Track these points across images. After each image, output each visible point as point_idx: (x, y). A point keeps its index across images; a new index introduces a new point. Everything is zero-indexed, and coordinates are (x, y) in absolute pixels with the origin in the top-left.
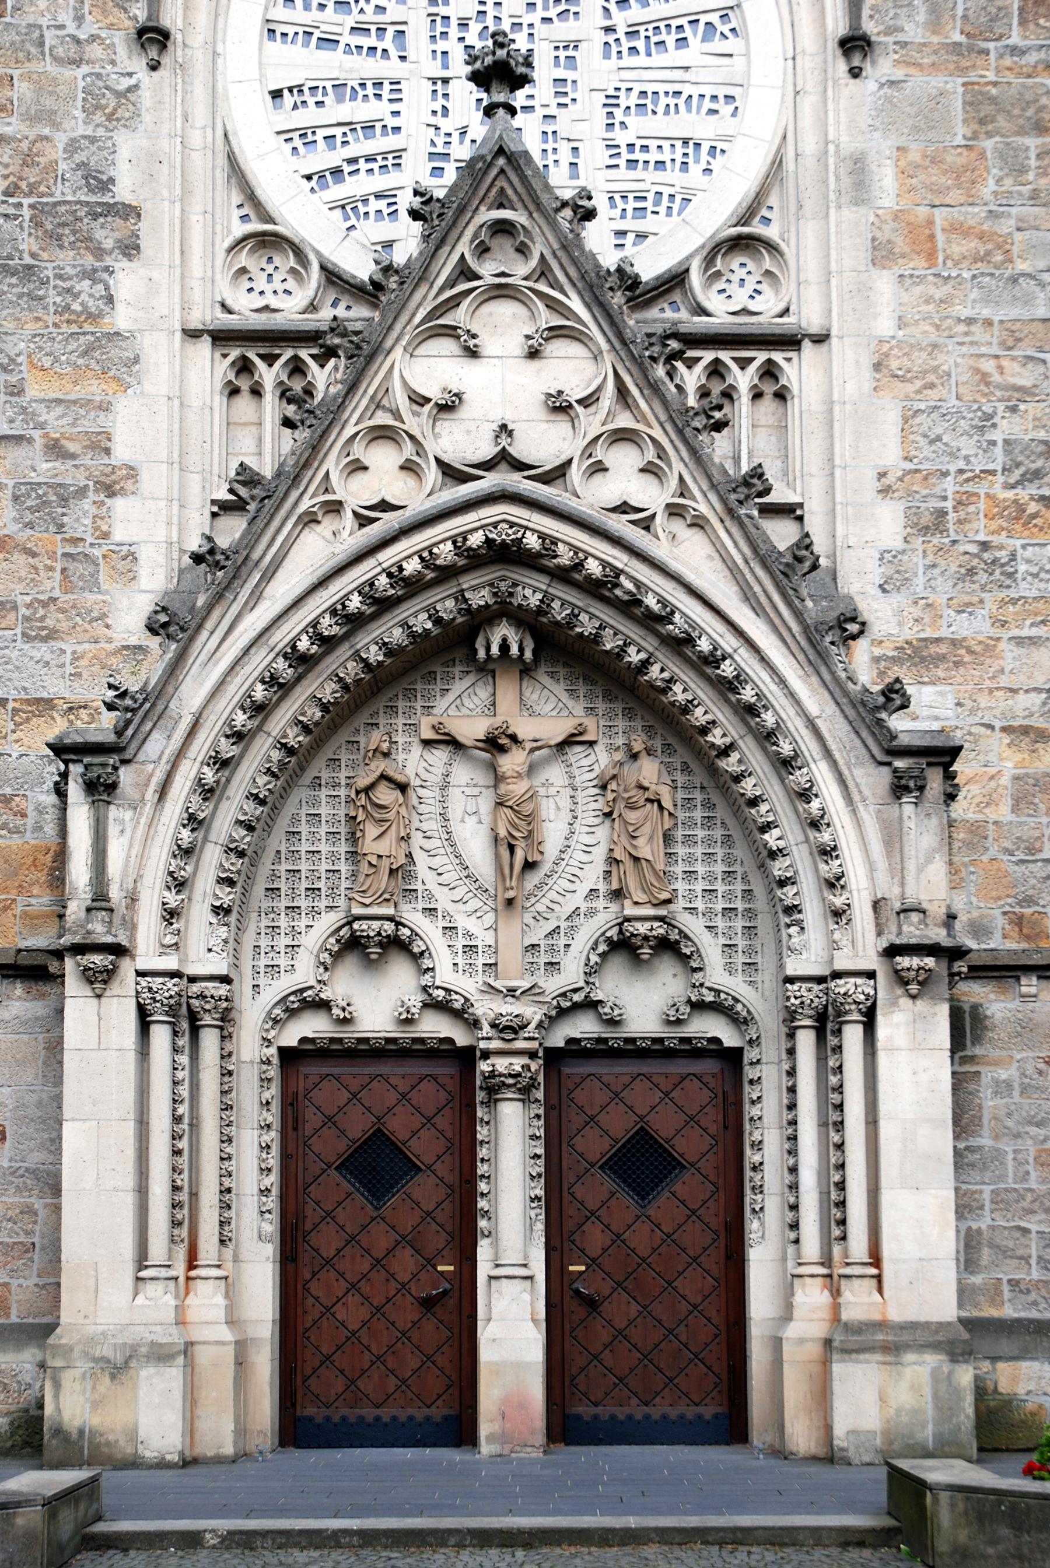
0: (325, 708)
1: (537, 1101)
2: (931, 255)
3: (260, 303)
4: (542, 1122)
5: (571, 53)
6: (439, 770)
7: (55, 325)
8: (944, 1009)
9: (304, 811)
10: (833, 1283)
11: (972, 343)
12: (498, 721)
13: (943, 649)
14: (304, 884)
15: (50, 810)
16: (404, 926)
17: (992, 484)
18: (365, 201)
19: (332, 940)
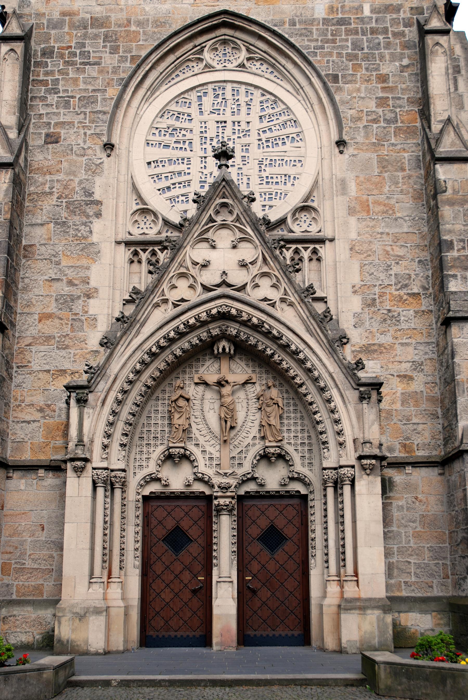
0: (161, 372)
1: (234, 515)
2: (368, 211)
3: (142, 232)
4: (236, 523)
5: (247, 147)
6: (200, 393)
7: (72, 241)
8: (379, 479)
9: (153, 409)
10: (341, 583)
11: (383, 241)
12: (221, 376)
13: (376, 347)
14: (153, 435)
15: (64, 409)
17: (391, 289)
18: (178, 197)
19: (162, 456)
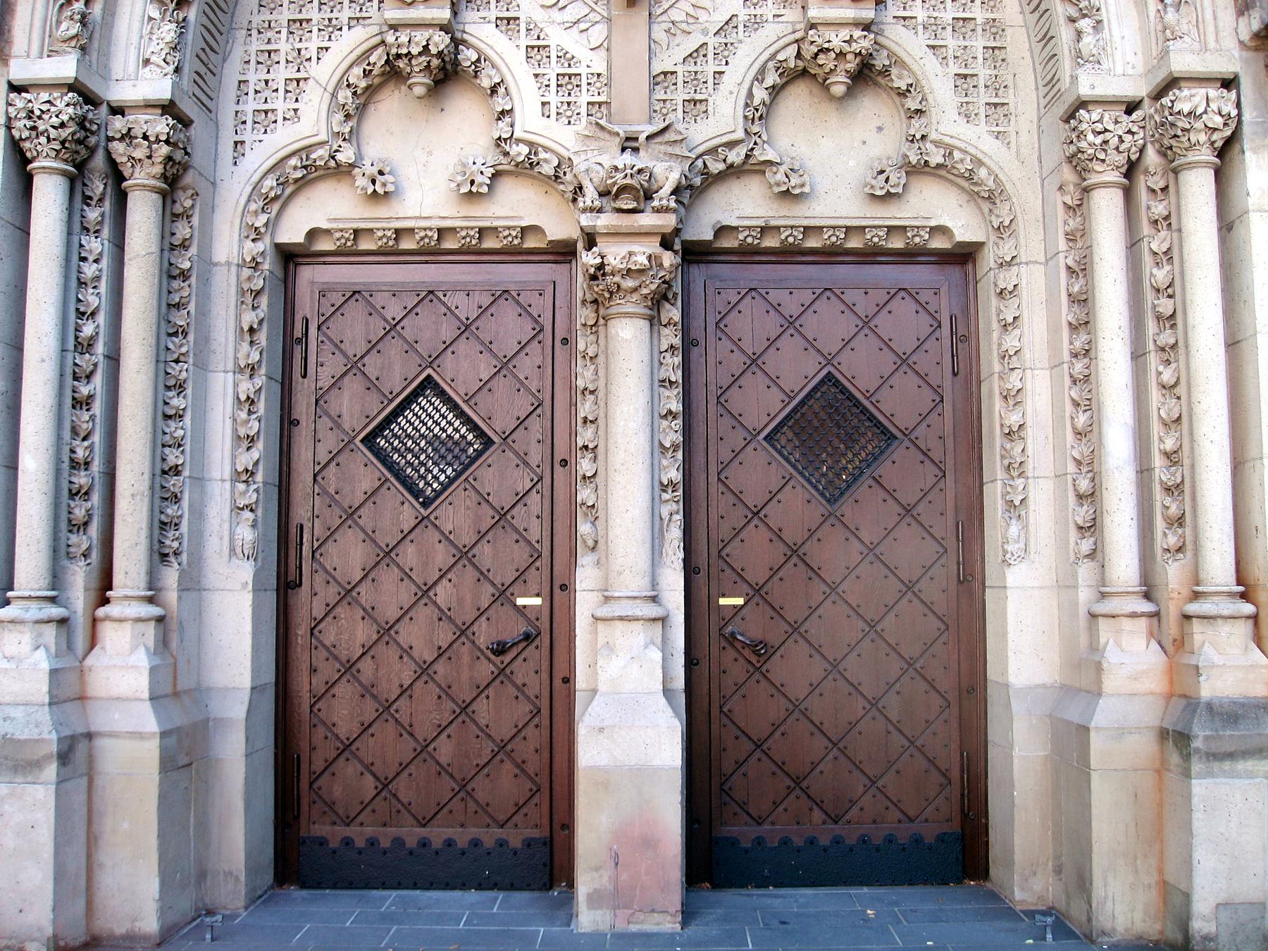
16: (469, 46)
19: (357, 71)
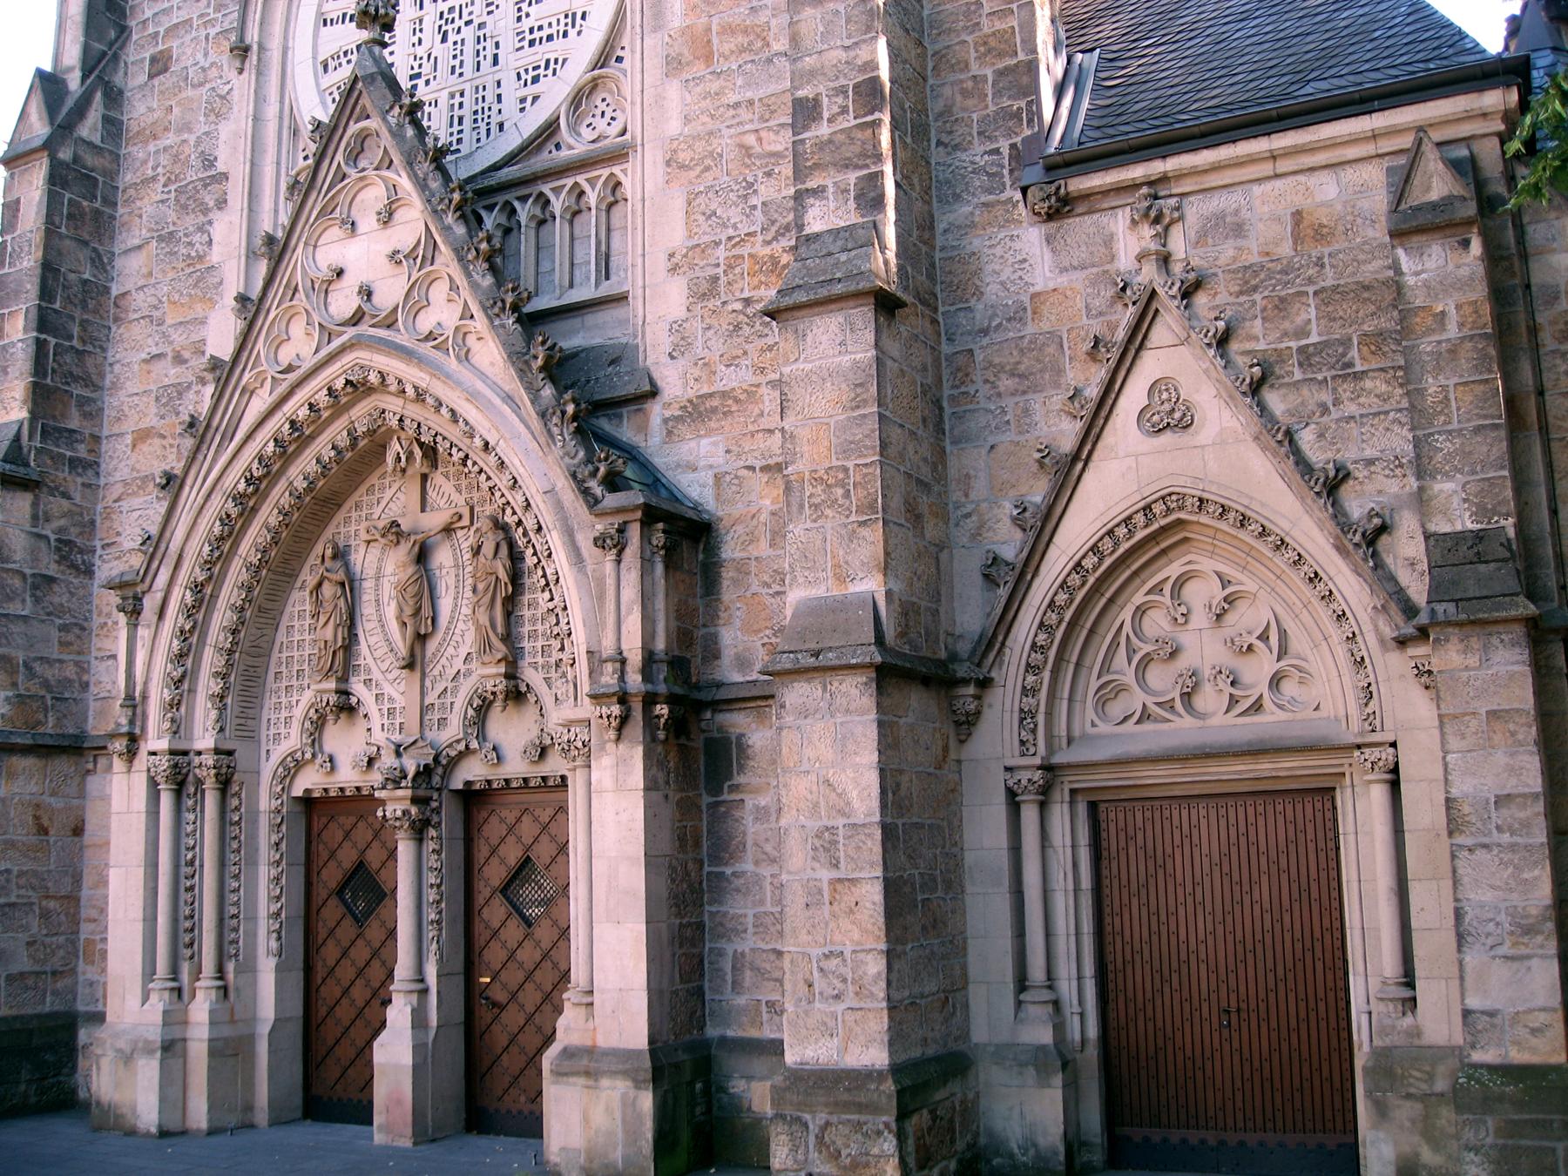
2: (708, 58)
13: (716, 402)
17: (753, 244)
